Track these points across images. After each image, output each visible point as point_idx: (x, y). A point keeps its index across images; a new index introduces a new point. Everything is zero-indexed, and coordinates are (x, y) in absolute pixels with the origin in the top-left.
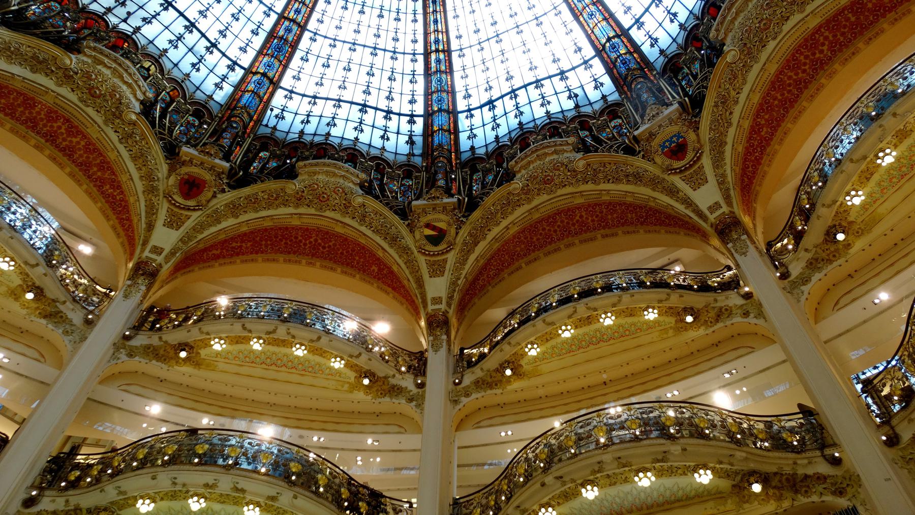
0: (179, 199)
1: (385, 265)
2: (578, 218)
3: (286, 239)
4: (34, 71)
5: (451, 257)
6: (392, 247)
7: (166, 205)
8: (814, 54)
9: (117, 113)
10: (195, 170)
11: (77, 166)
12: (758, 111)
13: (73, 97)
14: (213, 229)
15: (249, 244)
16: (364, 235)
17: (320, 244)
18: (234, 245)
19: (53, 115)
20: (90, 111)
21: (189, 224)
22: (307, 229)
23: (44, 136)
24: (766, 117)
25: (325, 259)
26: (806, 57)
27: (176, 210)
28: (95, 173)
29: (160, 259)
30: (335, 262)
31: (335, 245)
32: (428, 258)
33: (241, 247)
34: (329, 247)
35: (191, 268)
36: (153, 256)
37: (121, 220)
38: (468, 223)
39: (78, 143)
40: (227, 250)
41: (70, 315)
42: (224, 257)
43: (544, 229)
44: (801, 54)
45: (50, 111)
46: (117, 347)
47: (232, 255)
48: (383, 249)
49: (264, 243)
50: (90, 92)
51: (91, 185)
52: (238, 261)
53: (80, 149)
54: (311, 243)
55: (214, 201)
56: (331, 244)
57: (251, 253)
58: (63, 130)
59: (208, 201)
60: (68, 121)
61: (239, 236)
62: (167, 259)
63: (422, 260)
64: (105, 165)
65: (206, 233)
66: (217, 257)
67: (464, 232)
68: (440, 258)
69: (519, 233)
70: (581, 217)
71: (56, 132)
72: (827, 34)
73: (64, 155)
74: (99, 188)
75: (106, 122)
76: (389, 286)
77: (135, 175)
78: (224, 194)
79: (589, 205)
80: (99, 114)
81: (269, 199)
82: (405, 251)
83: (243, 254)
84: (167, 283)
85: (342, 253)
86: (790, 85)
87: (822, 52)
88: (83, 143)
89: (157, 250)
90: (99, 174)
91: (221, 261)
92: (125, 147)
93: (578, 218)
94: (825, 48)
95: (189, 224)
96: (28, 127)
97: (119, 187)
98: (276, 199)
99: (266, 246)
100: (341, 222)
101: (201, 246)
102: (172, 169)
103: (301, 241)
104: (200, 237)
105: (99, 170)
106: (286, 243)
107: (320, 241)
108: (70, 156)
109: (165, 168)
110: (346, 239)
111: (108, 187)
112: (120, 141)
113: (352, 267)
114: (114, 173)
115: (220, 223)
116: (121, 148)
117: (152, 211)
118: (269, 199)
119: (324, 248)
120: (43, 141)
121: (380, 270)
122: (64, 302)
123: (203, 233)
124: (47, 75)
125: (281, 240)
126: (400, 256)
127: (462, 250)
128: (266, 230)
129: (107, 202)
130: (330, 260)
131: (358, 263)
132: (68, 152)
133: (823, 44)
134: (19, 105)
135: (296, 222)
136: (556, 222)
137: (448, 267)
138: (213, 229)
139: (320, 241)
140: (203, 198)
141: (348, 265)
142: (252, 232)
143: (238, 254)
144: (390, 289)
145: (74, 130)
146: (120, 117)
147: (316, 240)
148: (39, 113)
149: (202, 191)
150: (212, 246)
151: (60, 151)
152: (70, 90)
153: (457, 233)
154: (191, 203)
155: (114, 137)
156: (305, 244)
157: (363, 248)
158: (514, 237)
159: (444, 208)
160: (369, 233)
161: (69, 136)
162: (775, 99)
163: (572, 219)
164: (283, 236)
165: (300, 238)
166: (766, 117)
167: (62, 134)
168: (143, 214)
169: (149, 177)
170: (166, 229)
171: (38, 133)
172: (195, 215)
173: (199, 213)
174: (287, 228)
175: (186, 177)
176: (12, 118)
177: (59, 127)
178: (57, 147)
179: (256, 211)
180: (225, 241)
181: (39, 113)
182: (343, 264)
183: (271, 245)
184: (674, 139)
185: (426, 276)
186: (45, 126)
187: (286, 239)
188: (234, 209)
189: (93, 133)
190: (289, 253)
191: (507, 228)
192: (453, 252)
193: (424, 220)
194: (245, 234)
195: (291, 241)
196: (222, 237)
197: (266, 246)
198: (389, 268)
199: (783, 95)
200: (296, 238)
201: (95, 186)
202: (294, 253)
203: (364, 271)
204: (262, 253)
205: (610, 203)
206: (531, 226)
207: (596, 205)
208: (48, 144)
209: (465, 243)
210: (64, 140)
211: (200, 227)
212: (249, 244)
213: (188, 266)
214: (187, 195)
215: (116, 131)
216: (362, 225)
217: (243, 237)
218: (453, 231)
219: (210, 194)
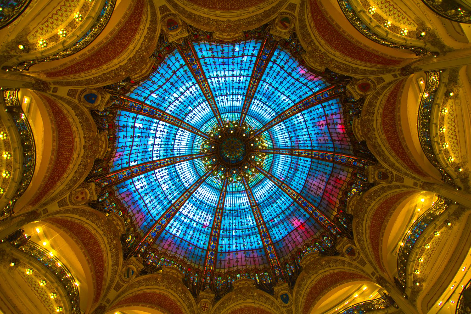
0: (372, 86)
1: (313, 18)
2: (221, 4)
4: (380, 146)
5: (283, 10)
6: (306, 25)
8: (115, 48)
12: (136, 31)
15: (361, 54)
16: (314, 35)
17: (335, 39)
18: (367, 58)
19: (386, 132)
20: (375, 126)
22: (335, 48)
24: (133, 27)
26: (117, 48)
27: (376, 83)
29: (397, 73)
30: (334, 28)
31: (329, 36)
32: (293, 13)
33: (365, 55)
35: (391, 58)
36: (398, 75)
37: (398, 90)
38: (269, 21)
39: (387, 120)
40: (371, 57)
42: (375, 55)
43: (237, 3)
44: (119, 50)
45: (386, 133)
47: (371, 53)
48: (310, 26)
54: (338, 41)
57: (363, 50)
59: (363, 79)
60: (384, 128)
63: (296, 14)
66: (377, 56)
67: (273, 17)
68: (288, 11)
69: (249, 7)
70: (219, 4)
72: (110, 55)
76: (317, 6)
79: (214, 8)
82: (302, 21)
84: (404, 59)
85: (328, 30)
86: (124, 38)
87: (112, 48)
89: (395, 76)
91: (377, 54)
93: (221, 4)
94: (110, 50)
99: (356, 49)
100: (320, 45)
101: (379, 66)
102: (366, 96)
103: (341, 44)
106: (347, 46)
110: (323, 36)
112: (374, 113)
113: (328, 22)
114: (385, 105)
115: (365, 70)
117: (384, 88)
119: (334, 36)
121: (317, 16)
124: (377, 142)
125: (348, 49)
126: (305, 19)
127: (277, 11)
128: (351, 56)
132: (393, 119)
133: (111, 51)
136: (231, 5)
137: (286, 6)
138: (369, 69)
142: (357, 58)
143: (369, 52)
144: (318, 4)
147: (335, 41)
148: (390, 134)
150: (375, 63)
153: (276, 18)
154: (369, 82)
156: (340, 42)
157: (318, 29)
158: (252, 6)
159: (276, 31)
161: (388, 123)
162: (129, 34)
163: (223, 4)
164: (347, 50)
166: (133, 27)
168: (388, 88)
169: (375, 97)
172: (371, 78)
173: (369, 77)
174: (343, 52)
177: (388, 127)
179: (349, 66)
180: (369, 61)
184: (172, 29)
185: (298, 6)
190: (349, 41)
191: (253, 12)
192: (281, 11)
193: (287, 31)
194: (360, 59)
196: (368, 64)
197: (356, 49)
198: (312, 15)
199: (126, 35)
200: (342, 46)
202: (347, 40)
203: (324, 18)
205: (205, 6)
206: (242, 8)
207: (211, 8)
209: (274, 12)
210: (390, 123)
212: (361, 54)
213: (390, 60)
218: (277, 21)
219: (360, 81)
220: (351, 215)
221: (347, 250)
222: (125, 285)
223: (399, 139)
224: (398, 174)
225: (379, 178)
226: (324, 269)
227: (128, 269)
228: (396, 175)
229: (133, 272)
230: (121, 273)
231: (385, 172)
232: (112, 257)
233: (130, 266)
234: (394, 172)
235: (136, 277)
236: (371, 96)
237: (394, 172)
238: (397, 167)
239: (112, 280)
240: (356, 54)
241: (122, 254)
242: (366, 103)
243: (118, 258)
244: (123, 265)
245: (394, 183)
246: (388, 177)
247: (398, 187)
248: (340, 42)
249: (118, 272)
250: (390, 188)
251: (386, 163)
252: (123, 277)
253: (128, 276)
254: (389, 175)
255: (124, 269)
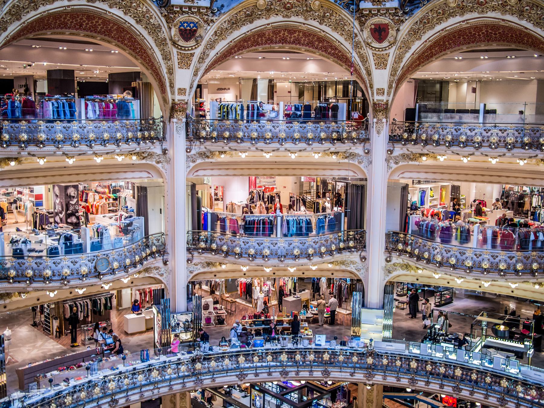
0: (376, 45)
3: (463, 36)
4: (251, 22)
7: (370, 52)
9: (308, 9)
10: (376, 20)
11: (306, 46)
13: (280, 18)
14: (408, 55)
18: (426, 54)
20: (293, 18)
21: (391, 60)
23: (280, 42)
25: (499, 41)
28: (318, 45)
34: (500, 33)
39: (299, 35)
41: (356, 151)
46: (387, 160)
49: (447, 43)
50: (286, 9)
51: (320, 52)
52: (434, 59)
53: (302, 38)
54: (483, 33)
55: (400, 34)
56: (500, 31)
57: (441, 52)
58: (286, 34)
61: (427, 49)
62: (389, 94)
64: (321, 39)
65: (404, 60)
66: (419, 65)
71: (284, 37)
73: (296, 44)
74: (326, 51)
75: (306, 19)
77: (341, 39)
78: (404, 24)
80: (300, 17)
81: (438, 16)
83: (435, 55)
88: (301, 34)
90: (321, 44)
92: (326, 25)
95: (391, 60)
96: (269, 44)
97: (336, 49)
98: (443, 14)
102: (362, 24)
103: (475, 34)
104: (402, 65)
105: (319, 43)
107: (490, 31)
108: (299, 43)
109: (356, 23)
111: (330, 50)
116: (323, 27)
118: (438, 16)
120: (281, 45)
122: (350, 149)
123: (402, 61)
124: (259, 18)
129: (335, 57)
130: (504, 41)
131: (527, 42)
132: (297, 41)
134: (258, 39)
135: (464, 25)
138: (408, 55)
139: (490, 31)
140: (390, 38)
141: (519, 43)
145: (291, 30)
146: (311, 10)
147: (487, 31)
148: (269, 35)
149: (388, 33)
151: (292, 44)
152: (275, 16)
154: (385, 44)
155: (315, 23)
160: (530, 26)
165: (473, 33)
167: (287, 36)
168: (360, 63)
169: (351, 36)
170: (378, 70)
171: (276, 43)
172: (392, 51)
173: (394, 47)
174: (460, 31)
175: (373, 27)
176: (259, 45)
177: (284, 34)
178: (289, 43)
181: (269, 35)
182: (515, 42)
183: (453, 42)
186: (276, 38)
187: (463, 36)
188: (415, 33)
189: (304, 28)
190: (469, 43)
194: (431, 46)
195: (467, 36)
197: (450, 44)
201: (322, 51)
204: (449, 49)
208: (284, 45)
210: (290, 38)
211: (399, 58)
212: (436, 49)
214: (380, 40)
215: (314, 19)
216: (522, 19)
217: (430, 48)
219: (394, 33)
223: (255, 46)
224: (195, 59)
225: (182, 24)
228: (192, 55)
231: (197, 35)
234: (198, 52)
236: (356, 31)
237: (198, 52)
238: (208, 55)
240: (442, 43)
242: (345, 14)
245: (175, 51)
246: (187, 39)
247: (167, 57)
248: (479, 35)
250: (161, 43)
251: (216, 32)
254: (192, 43)
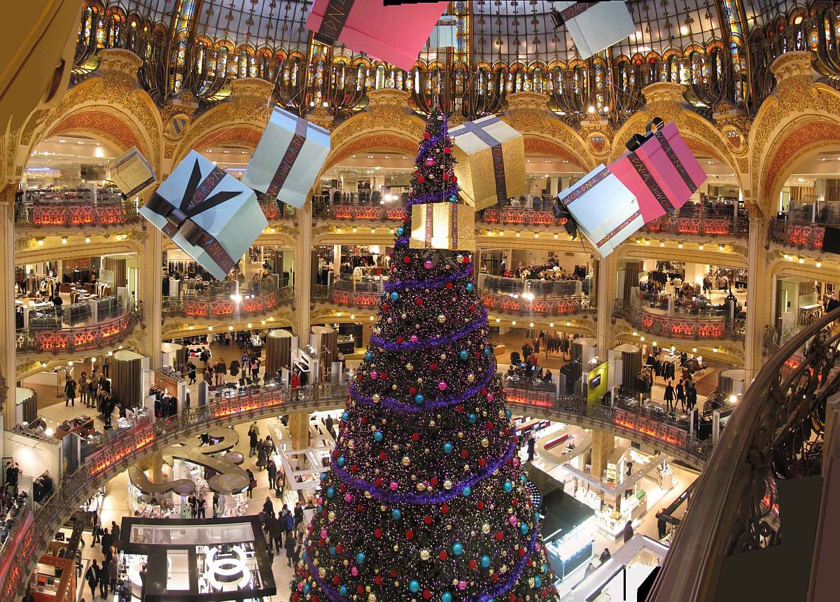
220: (645, 101)
221: (595, 138)
222: (179, 143)
226: (542, 133)
227: (175, 122)
229: (184, 122)
230: (166, 134)
232: (140, 119)
233: (176, 117)
235: (191, 123)
239: (157, 148)
241: (154, 106)
243: (150, 114)
244: (163, 119)
249: (161, 134)
252: (171, 136)
253: (178, 130)
255: (169, 125)
